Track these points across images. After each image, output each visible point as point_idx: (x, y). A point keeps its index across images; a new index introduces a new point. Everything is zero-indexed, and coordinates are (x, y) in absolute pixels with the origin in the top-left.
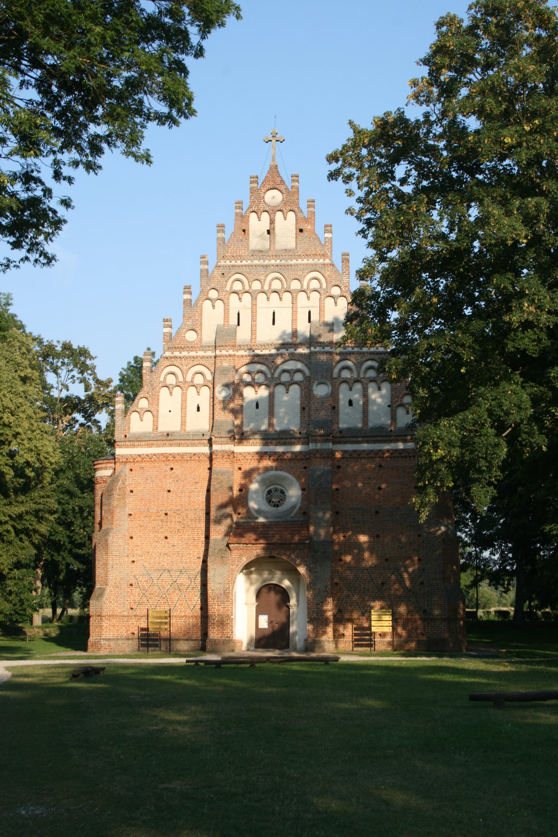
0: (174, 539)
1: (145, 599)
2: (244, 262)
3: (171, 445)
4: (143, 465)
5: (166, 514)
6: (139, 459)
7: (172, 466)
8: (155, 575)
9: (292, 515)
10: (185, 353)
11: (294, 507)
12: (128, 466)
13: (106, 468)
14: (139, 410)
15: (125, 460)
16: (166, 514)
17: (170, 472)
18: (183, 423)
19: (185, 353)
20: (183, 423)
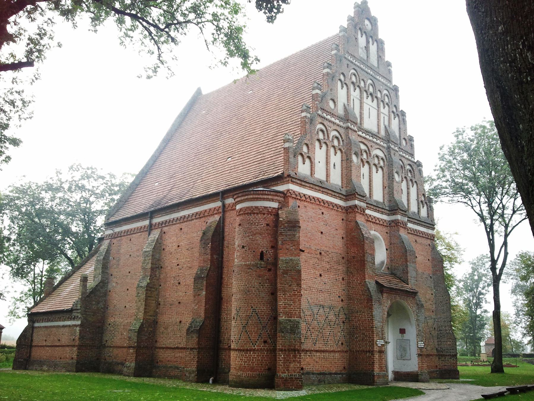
0: (325, 278)
1: (309, 333)
2: (357, 63)
3: (323, 192)
4: (306, 203)
5: (320, 253)
6: (303, 198)
7: (323, 211)
8: (315, 310)
9: (383, 269)
10: (329, 117)
11: (383, 263)
12: (298, 203)
13: (273, 200)
14: (303, 153)
15: (294, 196)
16: (320, 253)
17: (321, 216)
18: (328, 175)
19: (329, 117)
20: (328, 175)
